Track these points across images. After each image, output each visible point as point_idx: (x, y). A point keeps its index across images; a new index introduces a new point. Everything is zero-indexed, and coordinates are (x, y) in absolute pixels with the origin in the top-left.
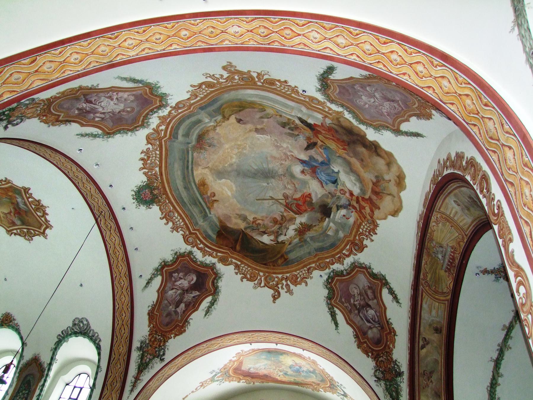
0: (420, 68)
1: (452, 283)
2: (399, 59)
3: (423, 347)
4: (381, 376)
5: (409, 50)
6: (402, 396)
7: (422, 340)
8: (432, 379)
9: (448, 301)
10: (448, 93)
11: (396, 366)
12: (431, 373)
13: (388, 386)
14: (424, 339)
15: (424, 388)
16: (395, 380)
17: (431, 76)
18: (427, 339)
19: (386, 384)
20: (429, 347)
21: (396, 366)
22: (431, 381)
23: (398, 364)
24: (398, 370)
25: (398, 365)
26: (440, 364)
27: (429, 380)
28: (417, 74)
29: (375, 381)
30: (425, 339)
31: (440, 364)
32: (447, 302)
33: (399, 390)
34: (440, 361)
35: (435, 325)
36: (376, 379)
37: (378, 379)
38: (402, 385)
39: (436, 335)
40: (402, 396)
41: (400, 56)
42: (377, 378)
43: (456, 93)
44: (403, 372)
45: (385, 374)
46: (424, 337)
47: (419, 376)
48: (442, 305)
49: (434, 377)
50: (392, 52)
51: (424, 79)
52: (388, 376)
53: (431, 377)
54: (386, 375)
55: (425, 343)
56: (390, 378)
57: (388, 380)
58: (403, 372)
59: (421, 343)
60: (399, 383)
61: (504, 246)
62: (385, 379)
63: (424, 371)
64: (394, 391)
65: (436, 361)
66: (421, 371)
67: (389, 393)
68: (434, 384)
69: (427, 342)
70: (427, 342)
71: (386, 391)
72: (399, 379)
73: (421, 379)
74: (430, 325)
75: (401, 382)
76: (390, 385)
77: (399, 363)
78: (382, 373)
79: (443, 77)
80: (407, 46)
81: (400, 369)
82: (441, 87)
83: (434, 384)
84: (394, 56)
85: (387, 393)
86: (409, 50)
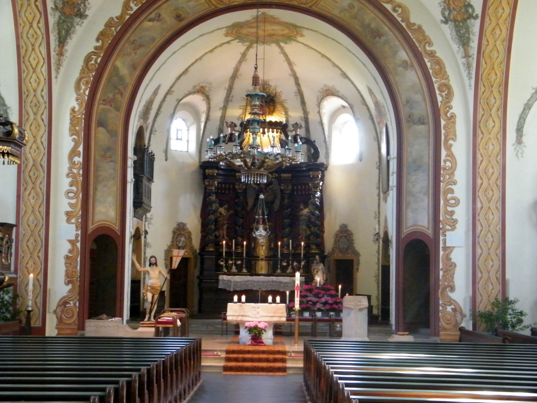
0: (498, 32)
1: (240, 3)
2: (499, 14)
3: (150, 20)
4: (60, 5)
5: (507, 22)
6: (71, 39)
7: (156, 14)
8: (138, 51)
9: (216, 7)
10: (490, 57)
11: (82, 5)
12: (141, 46)
13: (61, 21)
14: (158, 14)
15: (124, 55)
16: (72, 18)
17: (496, 42)
18: (161, 17)
19: (60, 18)
20: (156, 24)
21: (82, 5)
22: (136, 53)
23: (87, 4)
24: (82, 10)
25: (85, 5)
26: (155, 43)
27: (134, 50)
28: (493, 30)
29: (52, 8)
30: (160, 15)
31: (155, 43)
32: (213, 7)
33: (71, 31)
34: (156, 42)
35: (181, 12)
36: (54, 7)
37: (56, 8)
38: (77, 27)
39: (174, 19)
40: (71, 39)
41: (502, 15)
42: (56, 6)
43: (494, 64)
44: (87, 16)
45: (65, 6)
46: (161, 13)
47: (126, 42)
48: (207, 5)
49: (141, 51)
50: (503, 9)
51: (492, 36)
52: (67, 10)
53: (138, 49)
54: (65, 8)
55: (157, 18)
56: (68, 13)
57: (64, 13)
58: (87, 16)
59: (153, 16)
60: (75, 24)
61: (445, 136)
62: (63, 13)
63: (134, 41)
64: (65, 29)
65: (153, 40)
66: (132, 39)
67: (59, 29)
68: (137, 56)
69: (159, 18)
70: (159, 18)
71: (56, 25)
72: (77, 20)
73: (127, 45)
74: (177, 9)
75: (78, 24)
76: (64, 21)
77: (89, 4)
78: (63, 3)
79: (498, 51)
80: (509, 20)
81: (85, 11)
82: (491, 51)
83: (137, 56)
84: (500, 11)
85: (56, 28)
86: (507, 22)
